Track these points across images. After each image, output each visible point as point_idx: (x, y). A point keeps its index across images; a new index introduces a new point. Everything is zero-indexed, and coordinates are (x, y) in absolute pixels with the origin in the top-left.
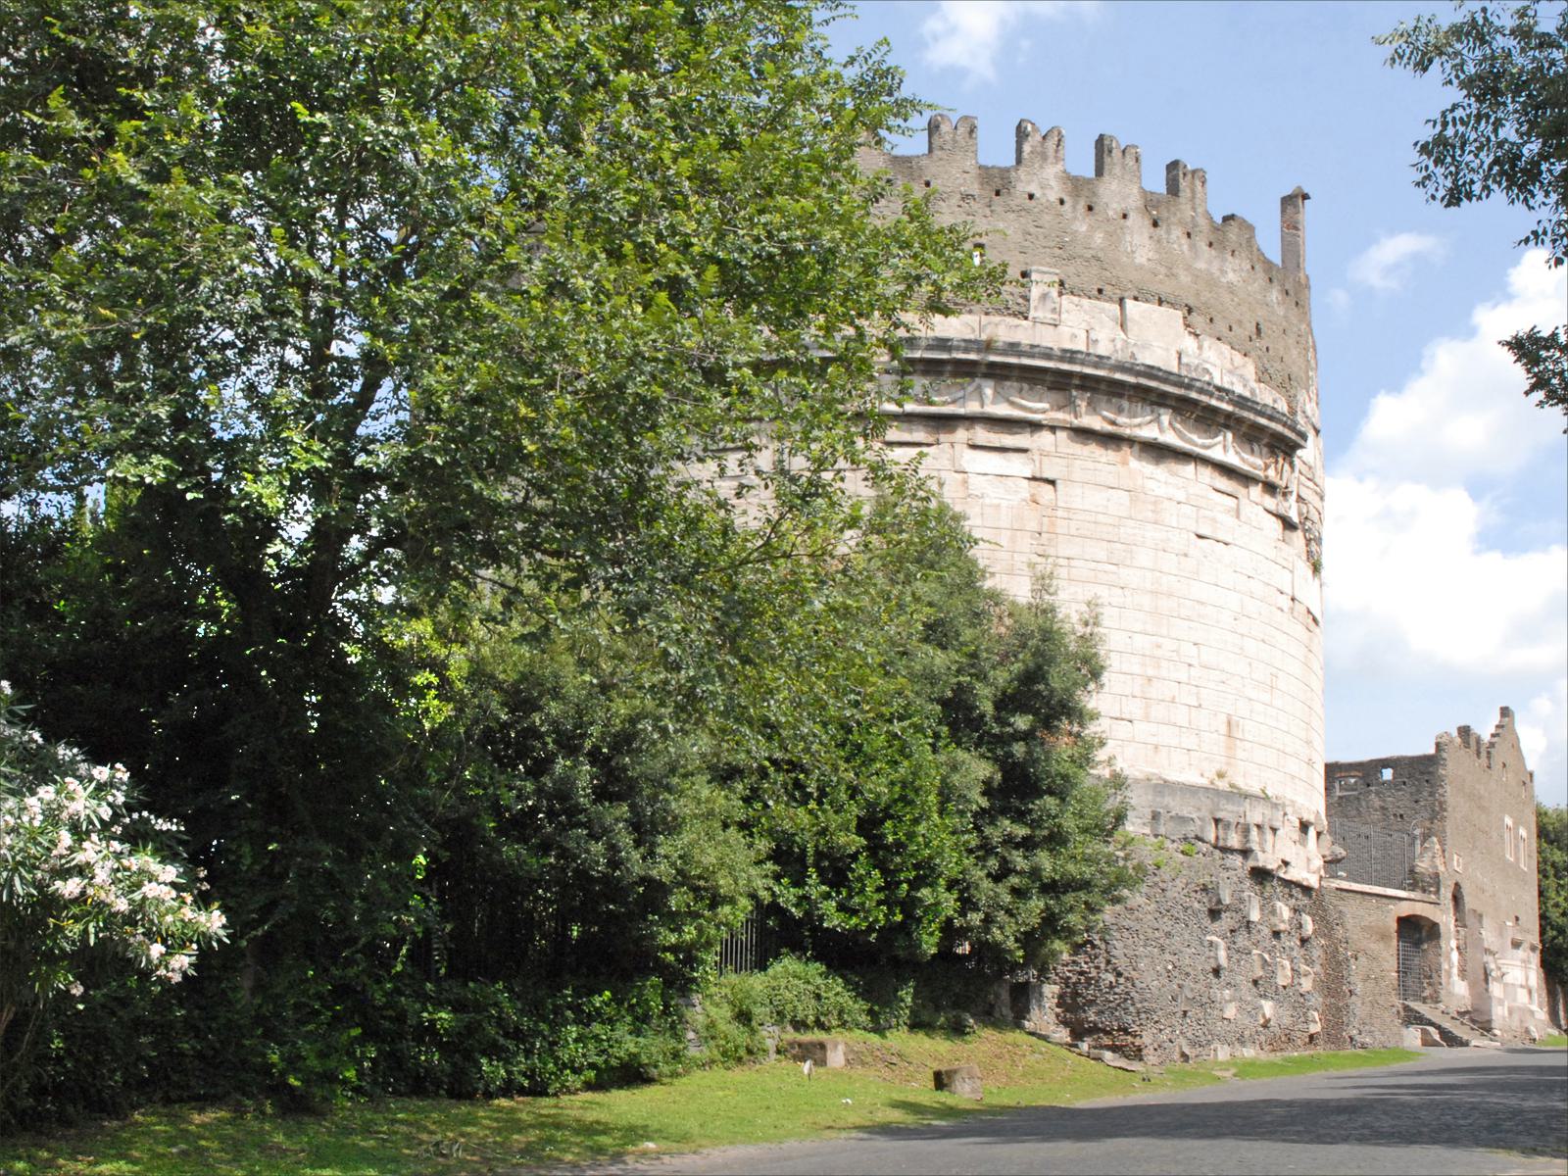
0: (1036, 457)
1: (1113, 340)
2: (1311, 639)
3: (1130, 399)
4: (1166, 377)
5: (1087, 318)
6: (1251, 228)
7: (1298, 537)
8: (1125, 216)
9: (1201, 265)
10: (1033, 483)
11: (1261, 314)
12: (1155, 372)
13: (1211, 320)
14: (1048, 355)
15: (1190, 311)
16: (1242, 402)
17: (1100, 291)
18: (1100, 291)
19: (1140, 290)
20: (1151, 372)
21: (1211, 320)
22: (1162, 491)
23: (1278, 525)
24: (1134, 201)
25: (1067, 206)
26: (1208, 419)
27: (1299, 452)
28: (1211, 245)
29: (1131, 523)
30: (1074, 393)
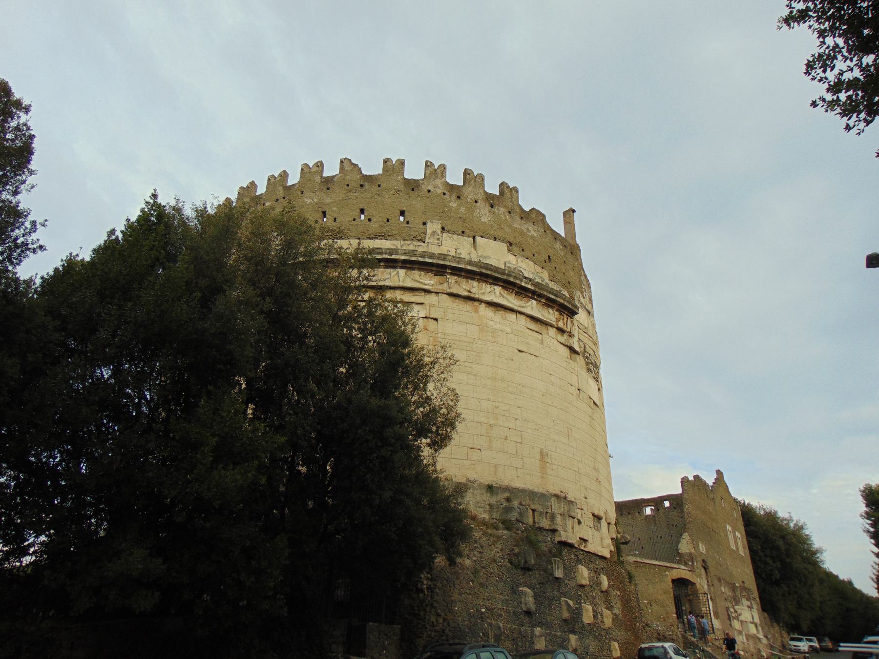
0: (427, 307)
1: (470, 254)
2: (593, 413)
3: (478, 280)
4: (497, 269)
5: (456, 243)
6: (544, 216)
7: (580, 359)
8: (476, 202)
9: (516, 225)
10: (425, 319)
11: (551, 252)
12: (490, 267)
13: (523, 250)
14: (432, 256)
15: (511, 244)
16: (537, 285)
17: (463, 232)
18: (463, 232)
19: (483, 233)
20: (487, 266)
21: (523, 250)
22: (498, 326)
23: (566, 352)
24: (480, 196)
25: (447, 196)
26: (521, 291)
27: (576, 316)
28: (521, 218)
29: (480, 342)
30: (448, 276)
